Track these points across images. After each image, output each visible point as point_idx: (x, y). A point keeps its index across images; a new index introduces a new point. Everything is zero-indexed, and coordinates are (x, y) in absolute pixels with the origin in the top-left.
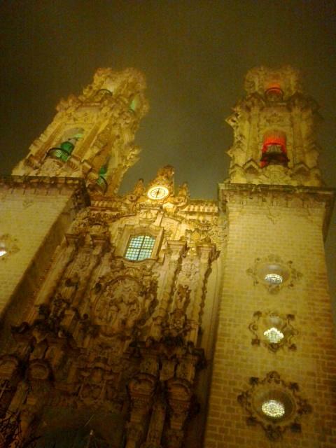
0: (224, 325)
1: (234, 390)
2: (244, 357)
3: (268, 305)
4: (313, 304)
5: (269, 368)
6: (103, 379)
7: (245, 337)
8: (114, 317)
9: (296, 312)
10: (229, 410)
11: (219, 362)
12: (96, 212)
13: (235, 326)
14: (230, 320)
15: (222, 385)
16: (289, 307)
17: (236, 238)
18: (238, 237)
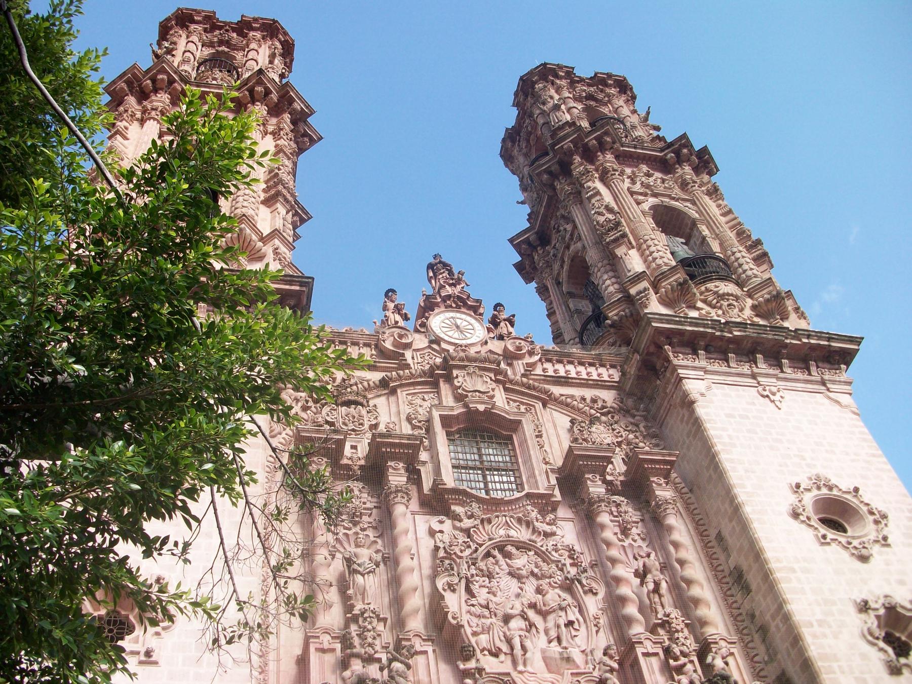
0: (815, 636)
7: (864, 656)
8: (528, 643)
13: (836, 637)
14: (821, 623)
16: (901, 582)
17: (727, 440)
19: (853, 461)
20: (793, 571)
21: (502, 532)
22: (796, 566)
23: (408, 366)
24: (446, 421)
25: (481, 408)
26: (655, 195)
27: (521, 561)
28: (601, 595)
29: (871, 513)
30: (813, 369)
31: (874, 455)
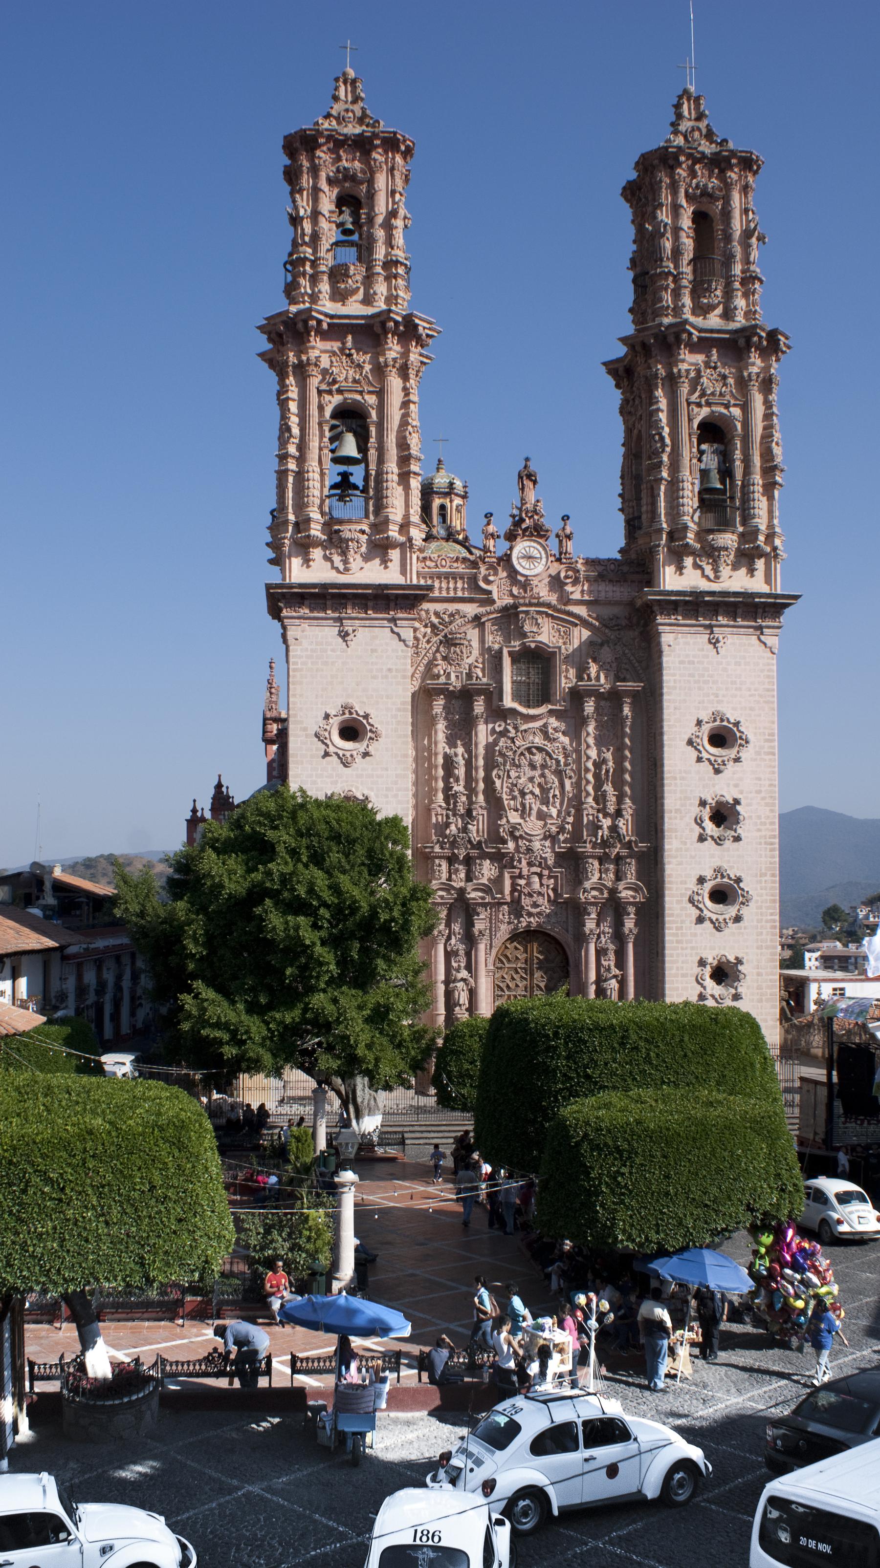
0: (670, 818)
1: (686, 889)
2: (693, 853)
3: (714, 785)
4: (759, 779)
5: (717, 863)
6: (542, 885)
9: (741, 792)
10: (682, 909)
11: (669, 863)
12: (439, 607)
13: (681, 819)
14: (677, 811)
15: (674, 886)
16: (736, 786)
18: (675, 681)
19: (750, 696)
20: (675, 779)
21: (531, 738)
22: (678, 776)
23: (493, 602)
24: (510, 654)
25: (533, 645)
26: (708, 404)
27: (538, 758)
28: (574, 780)
29: (741, 738)
30: (759, 615)
31: (768, 690)
